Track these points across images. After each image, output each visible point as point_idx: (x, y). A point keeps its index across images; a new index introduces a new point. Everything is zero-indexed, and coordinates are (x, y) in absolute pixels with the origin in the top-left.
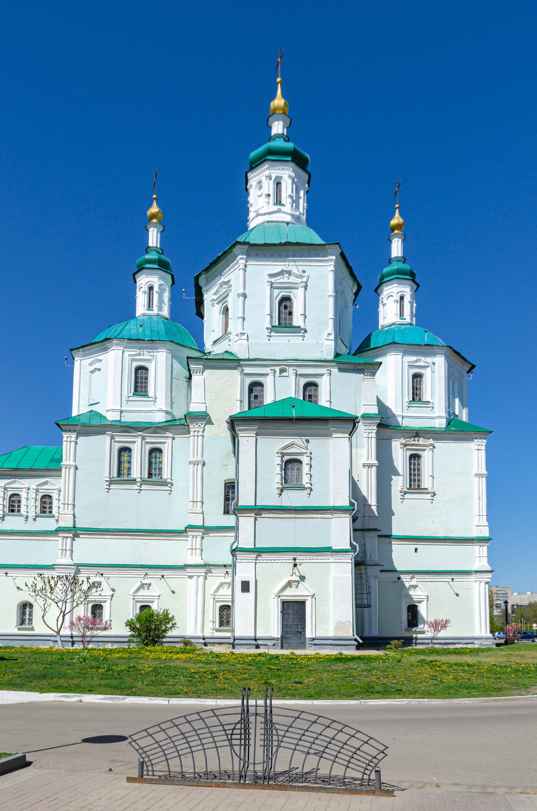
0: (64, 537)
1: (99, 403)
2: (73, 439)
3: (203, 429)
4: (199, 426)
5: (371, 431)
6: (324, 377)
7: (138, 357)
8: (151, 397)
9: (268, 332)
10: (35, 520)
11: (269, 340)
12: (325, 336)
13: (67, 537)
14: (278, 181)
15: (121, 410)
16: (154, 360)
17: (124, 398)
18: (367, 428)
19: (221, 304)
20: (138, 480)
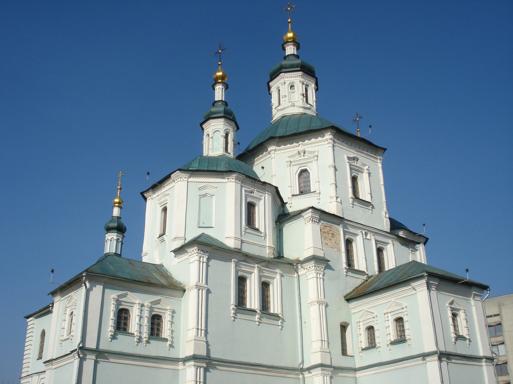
0: (198, 366)
2: (205, 260)
3: (323, 273)
6: (389, 246)
7: (250, 194)
8: (261, 233)
9: (352, 201)
10: (148, 342)
11: (353, 207)
12: (383, 214)
13: (200, 367)
15: (242, 240)
16: (262, 201)
17: (243, 230)
19: (298, 166)
20: (258, 311)
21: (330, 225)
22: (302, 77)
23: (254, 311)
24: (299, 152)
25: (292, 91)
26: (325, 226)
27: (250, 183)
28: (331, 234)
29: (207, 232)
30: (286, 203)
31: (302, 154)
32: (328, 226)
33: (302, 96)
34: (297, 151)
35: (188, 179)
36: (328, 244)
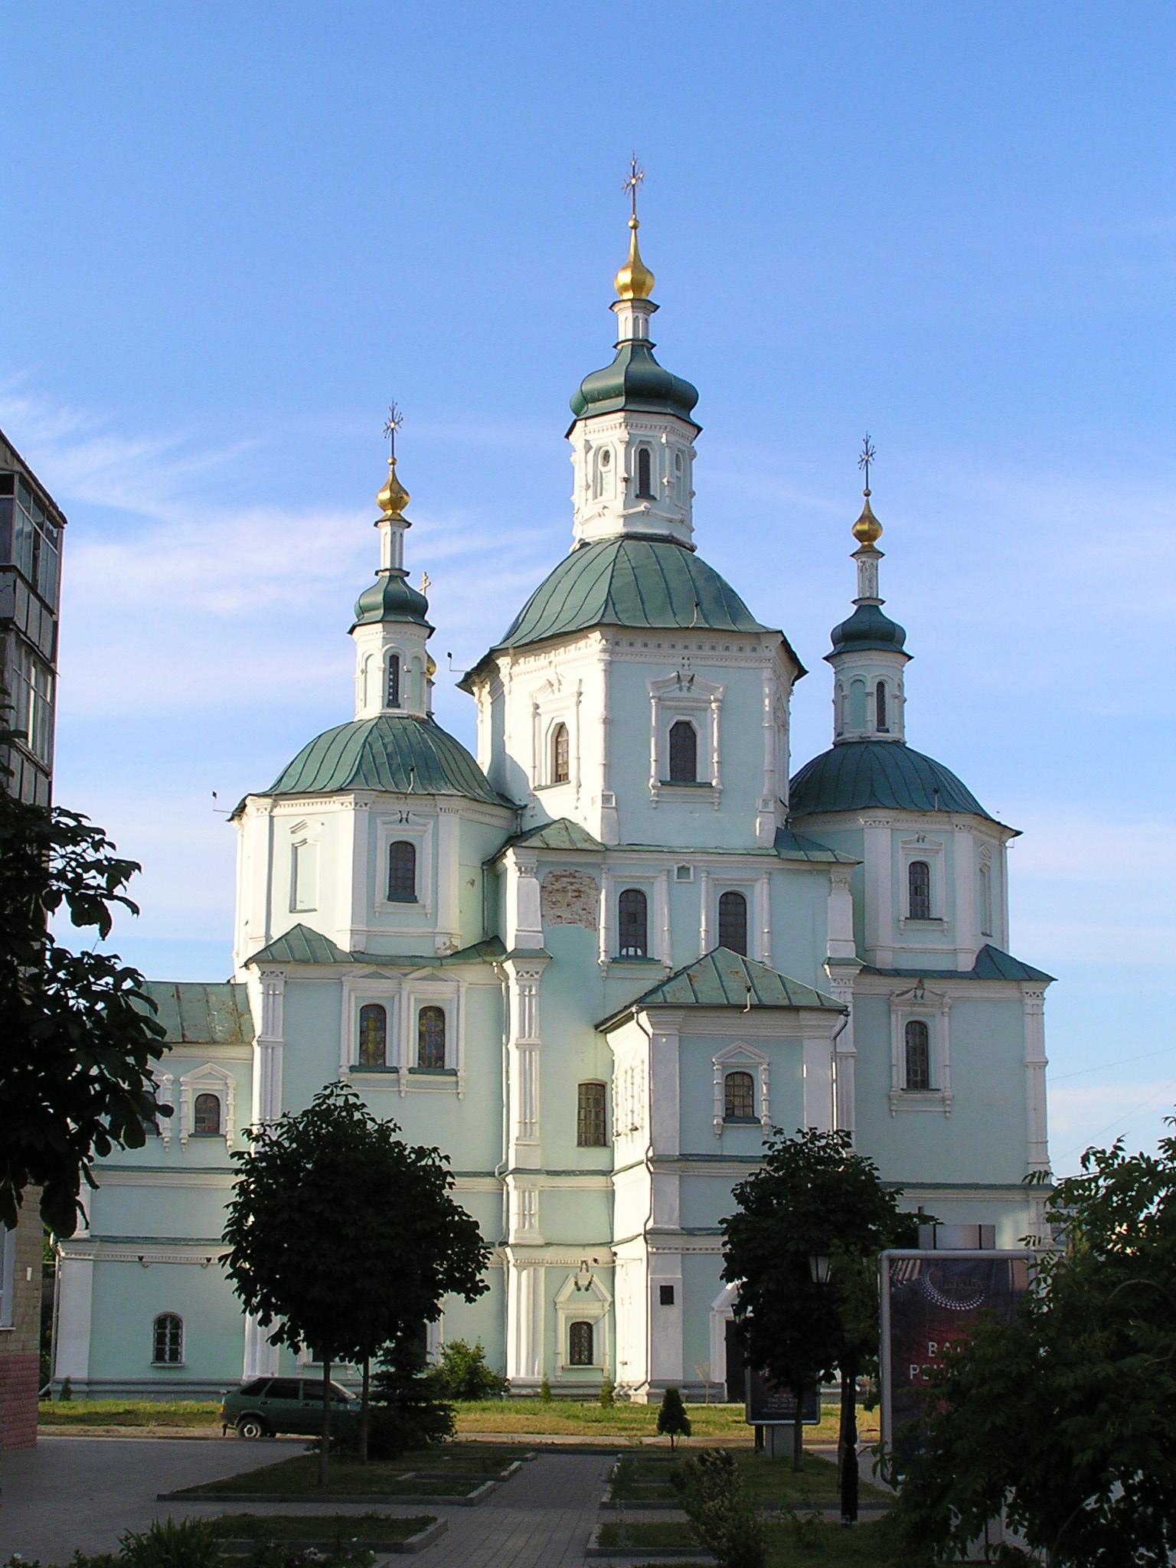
1: (315, 910)
4: (532, 976)
5: (843, 990)
12: (759, 803)
14: (644, 447)
18: (836, 985)
21: (573, 872)
22: (626, 426)
23: (395, 1070)
24: (550, 682)
25: (603, 469)
26: (558, 878)
27: (395, 800)
28: (574, 891)
29: (309, 921)
30: (526, 806)
31: (556, 685)
32: (564, 876)
33: (624, 483)
34: (544, 681)
35: (271, 811)
36: (564, 916)
